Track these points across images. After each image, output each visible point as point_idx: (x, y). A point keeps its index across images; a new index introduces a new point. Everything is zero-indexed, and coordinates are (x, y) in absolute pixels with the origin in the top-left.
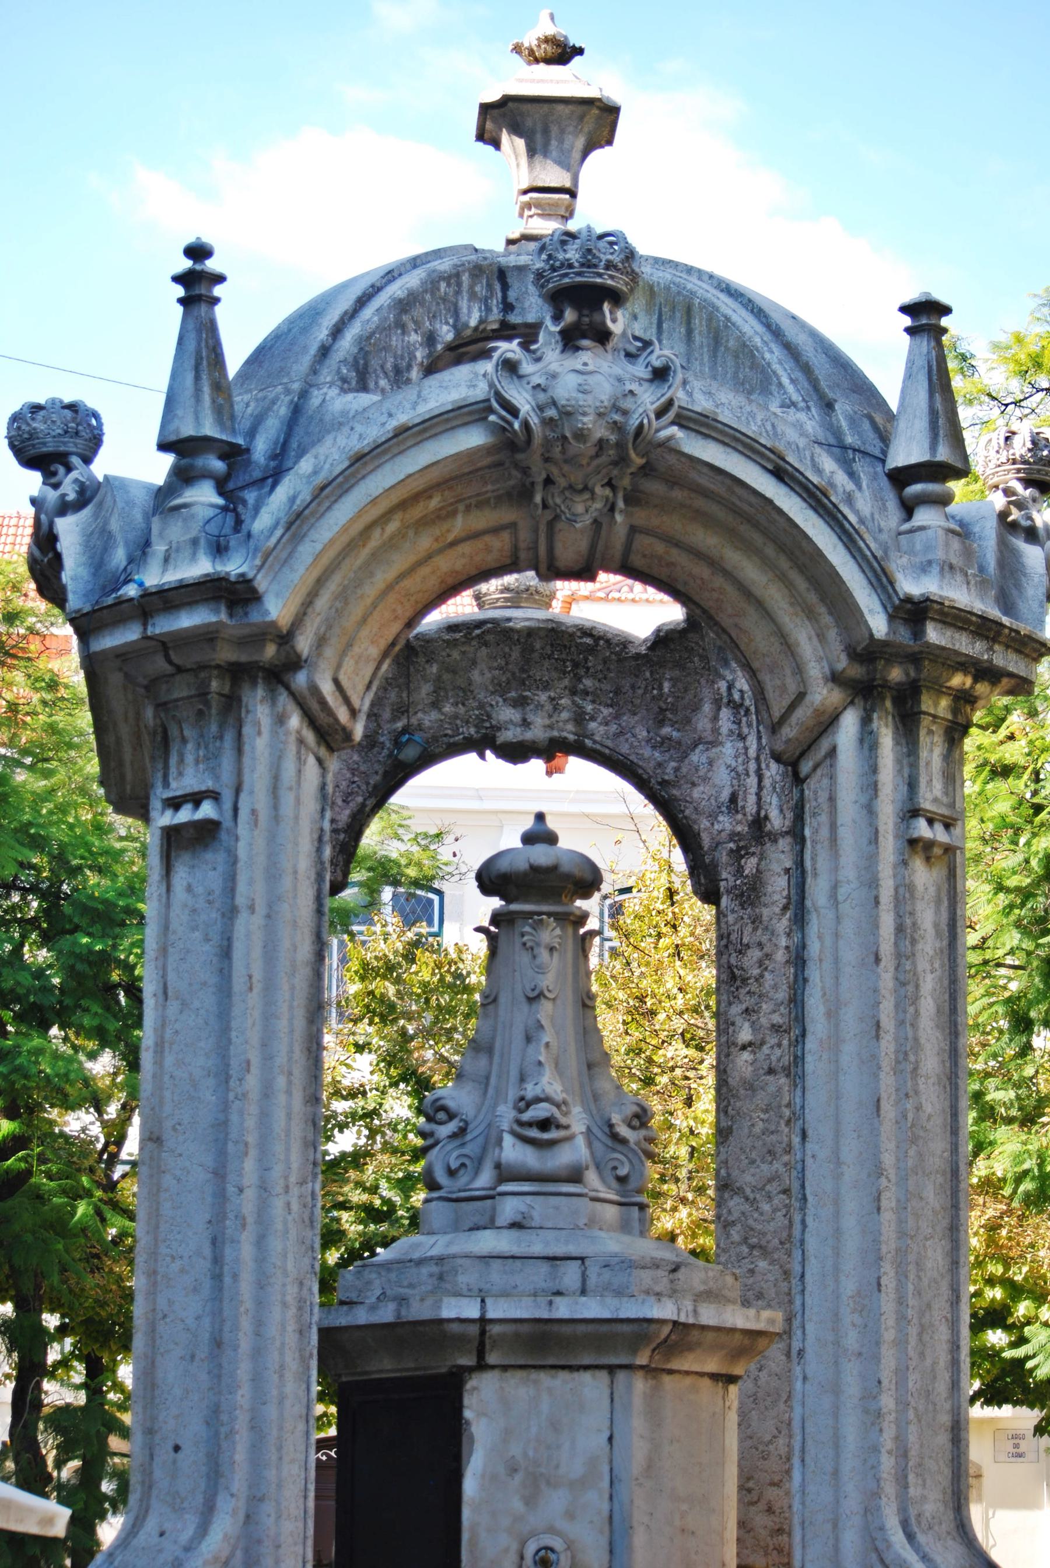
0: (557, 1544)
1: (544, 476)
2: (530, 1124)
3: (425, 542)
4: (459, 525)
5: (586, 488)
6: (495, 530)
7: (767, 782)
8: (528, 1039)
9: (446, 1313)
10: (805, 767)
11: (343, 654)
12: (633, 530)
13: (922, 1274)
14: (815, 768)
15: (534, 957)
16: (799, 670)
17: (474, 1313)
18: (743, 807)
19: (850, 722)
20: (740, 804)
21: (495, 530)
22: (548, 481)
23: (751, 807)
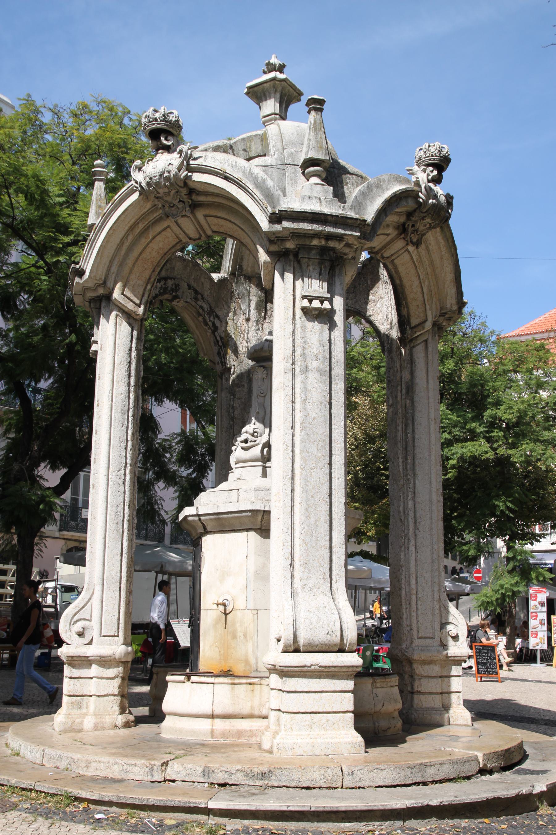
0: (229, 598)
6: (165, 229)
13: (308, 484)
21: (165, 229)
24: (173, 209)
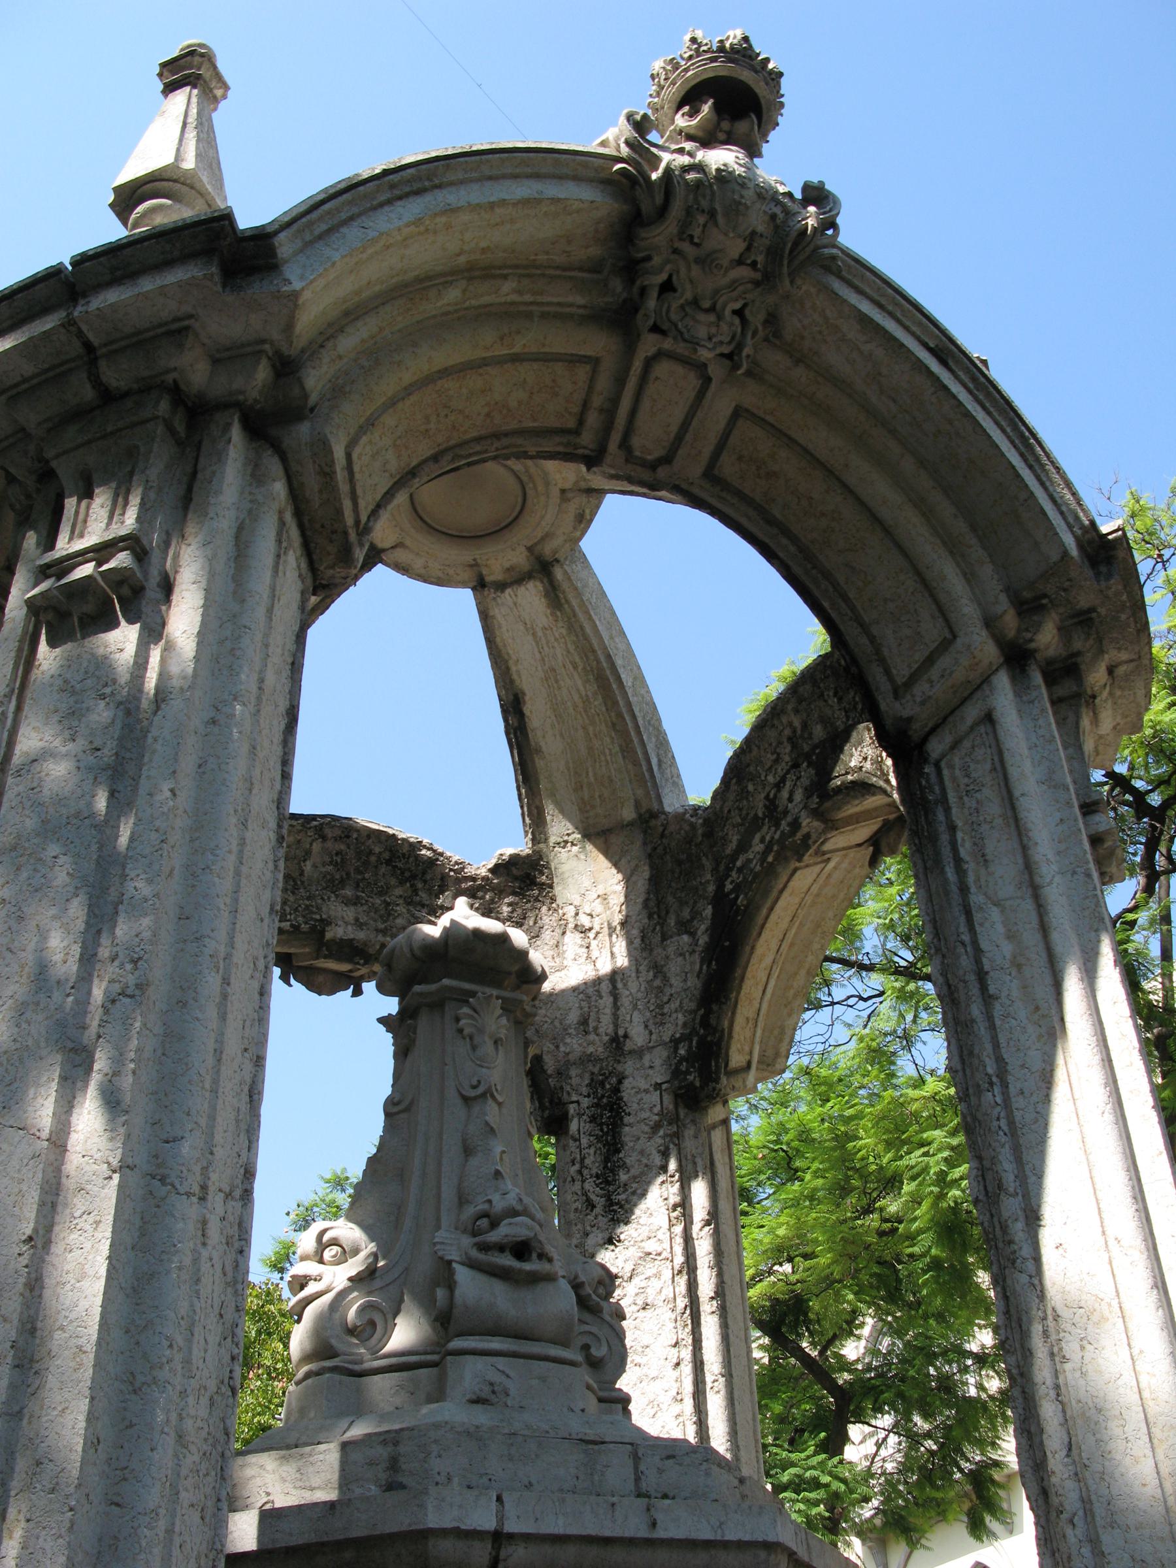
1: (664, 277)
2: (501, 1248)
3: (485, 341)
4: (527, 340)
5: (712, 309)
7: (625, 1001)
8: (468, 1151)
9: (433, 1520)
10: (936, 747)
11: (362, 430)
12: (738, 413)
14: (955, 746)
15: (474, 1048)
16: (942, 612)
17: (485, 1520)
18: (596, 1029)
19: (1003, 681)
20: (592, 1024)
21: (573, 360)
22: (667, 287)
23: (606, 1025)
24: (702, 317)
